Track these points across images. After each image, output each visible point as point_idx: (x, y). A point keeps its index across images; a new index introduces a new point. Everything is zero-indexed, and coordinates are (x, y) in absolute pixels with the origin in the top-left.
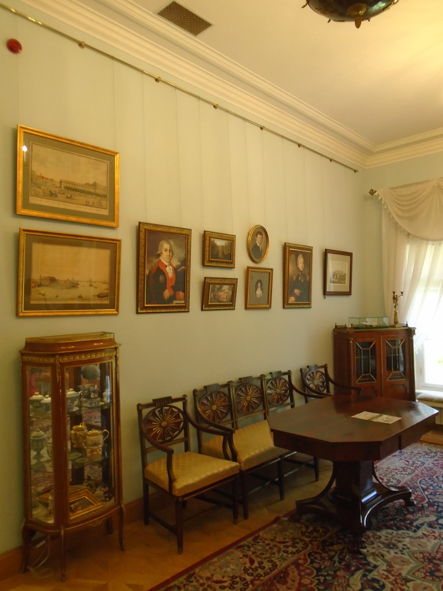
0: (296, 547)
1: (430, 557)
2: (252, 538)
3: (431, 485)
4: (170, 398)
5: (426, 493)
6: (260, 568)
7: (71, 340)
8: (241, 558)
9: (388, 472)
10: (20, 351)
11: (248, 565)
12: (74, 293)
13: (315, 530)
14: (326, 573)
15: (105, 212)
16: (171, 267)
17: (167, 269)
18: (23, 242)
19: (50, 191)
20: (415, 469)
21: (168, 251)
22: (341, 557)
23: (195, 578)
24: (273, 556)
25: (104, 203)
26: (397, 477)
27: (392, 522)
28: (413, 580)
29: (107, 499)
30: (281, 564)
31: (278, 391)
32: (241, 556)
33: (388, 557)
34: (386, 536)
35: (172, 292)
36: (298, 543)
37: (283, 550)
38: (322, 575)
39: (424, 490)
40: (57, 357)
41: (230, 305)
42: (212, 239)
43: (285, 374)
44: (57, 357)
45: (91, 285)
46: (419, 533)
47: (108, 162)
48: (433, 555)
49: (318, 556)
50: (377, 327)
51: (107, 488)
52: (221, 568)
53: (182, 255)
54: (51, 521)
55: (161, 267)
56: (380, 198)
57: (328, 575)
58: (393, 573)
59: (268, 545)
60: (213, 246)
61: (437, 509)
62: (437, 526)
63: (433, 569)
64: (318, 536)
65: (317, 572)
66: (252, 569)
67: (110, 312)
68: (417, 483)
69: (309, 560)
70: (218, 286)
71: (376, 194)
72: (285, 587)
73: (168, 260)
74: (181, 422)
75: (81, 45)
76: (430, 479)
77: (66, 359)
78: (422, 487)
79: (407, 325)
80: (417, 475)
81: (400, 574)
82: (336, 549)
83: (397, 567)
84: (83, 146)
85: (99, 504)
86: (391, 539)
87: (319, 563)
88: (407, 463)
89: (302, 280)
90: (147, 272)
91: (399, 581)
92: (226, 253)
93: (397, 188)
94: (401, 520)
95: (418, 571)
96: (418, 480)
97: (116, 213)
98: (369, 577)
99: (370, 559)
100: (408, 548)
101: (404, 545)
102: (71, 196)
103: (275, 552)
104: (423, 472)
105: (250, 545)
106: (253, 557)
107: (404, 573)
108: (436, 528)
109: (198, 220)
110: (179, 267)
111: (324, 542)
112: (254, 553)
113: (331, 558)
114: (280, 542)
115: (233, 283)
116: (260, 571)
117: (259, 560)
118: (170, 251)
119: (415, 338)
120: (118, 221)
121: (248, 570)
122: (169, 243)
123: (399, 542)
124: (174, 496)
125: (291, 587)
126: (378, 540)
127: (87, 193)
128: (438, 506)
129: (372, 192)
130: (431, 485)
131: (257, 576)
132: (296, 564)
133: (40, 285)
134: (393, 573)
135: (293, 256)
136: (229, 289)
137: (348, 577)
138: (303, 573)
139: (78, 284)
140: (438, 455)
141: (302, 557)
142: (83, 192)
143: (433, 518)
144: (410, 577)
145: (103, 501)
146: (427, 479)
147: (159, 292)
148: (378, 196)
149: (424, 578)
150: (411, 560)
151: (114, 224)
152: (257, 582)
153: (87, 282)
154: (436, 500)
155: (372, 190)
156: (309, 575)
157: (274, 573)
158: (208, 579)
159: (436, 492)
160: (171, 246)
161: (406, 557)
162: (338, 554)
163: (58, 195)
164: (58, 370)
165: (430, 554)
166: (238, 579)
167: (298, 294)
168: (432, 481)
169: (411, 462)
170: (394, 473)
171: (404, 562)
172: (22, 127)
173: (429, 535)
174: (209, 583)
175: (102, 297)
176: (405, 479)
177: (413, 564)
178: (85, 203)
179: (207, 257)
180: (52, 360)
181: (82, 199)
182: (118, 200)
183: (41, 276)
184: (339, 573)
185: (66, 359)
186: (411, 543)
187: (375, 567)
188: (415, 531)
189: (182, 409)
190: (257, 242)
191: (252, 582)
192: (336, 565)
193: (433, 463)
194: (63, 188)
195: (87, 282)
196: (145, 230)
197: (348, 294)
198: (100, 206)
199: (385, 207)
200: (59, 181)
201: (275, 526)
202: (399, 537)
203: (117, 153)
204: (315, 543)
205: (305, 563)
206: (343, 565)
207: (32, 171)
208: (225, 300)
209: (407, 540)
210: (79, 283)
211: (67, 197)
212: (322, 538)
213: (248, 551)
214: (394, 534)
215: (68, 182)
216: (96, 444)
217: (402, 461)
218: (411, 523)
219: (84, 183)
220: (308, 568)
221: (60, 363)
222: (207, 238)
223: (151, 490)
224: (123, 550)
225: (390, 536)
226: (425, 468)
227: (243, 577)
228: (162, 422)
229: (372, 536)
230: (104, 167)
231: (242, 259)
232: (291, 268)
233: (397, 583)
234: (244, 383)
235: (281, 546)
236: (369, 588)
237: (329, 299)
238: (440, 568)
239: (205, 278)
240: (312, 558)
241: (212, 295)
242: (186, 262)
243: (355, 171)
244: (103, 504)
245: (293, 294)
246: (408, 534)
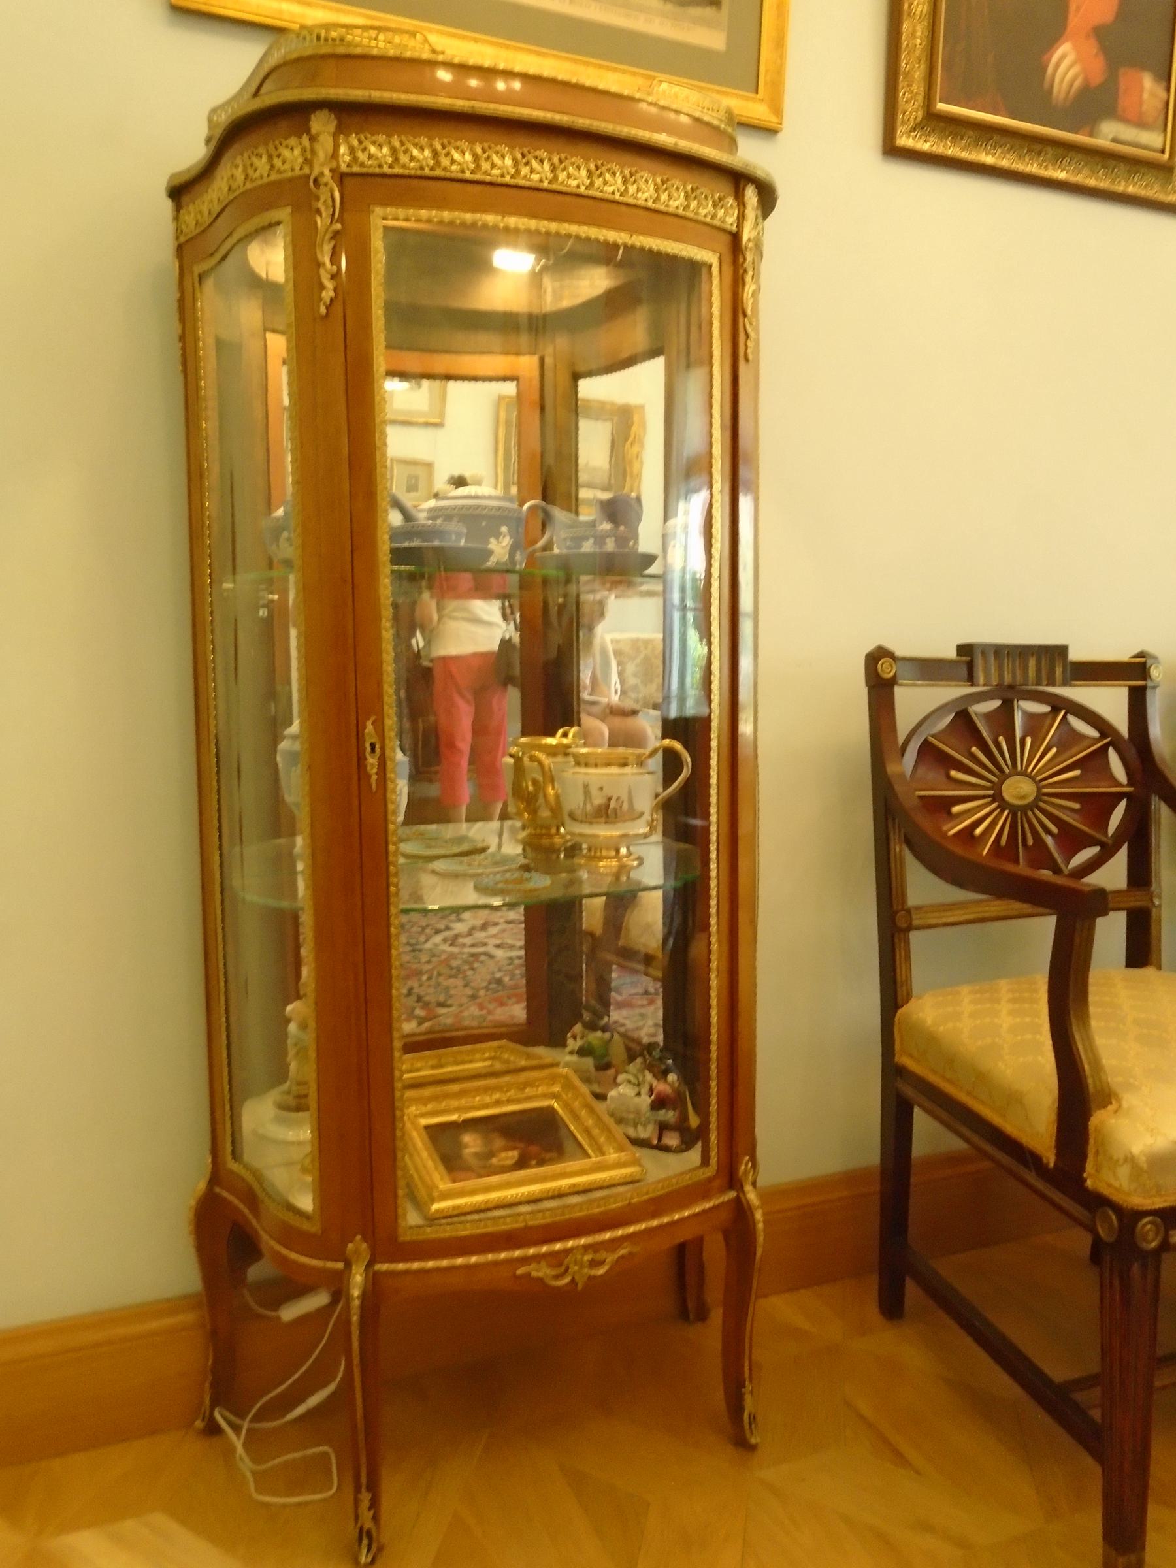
4: (1056, 653)
29: (672, 1140)
35: (1098, 69)
40: (322, 124)
51: (672, 1077)
54: (306, 1202)
74: (1113, 800)
85: (613, 1156)
124: (1098, 1202)
189: (1121, 722)
216: (606, 813)
221: (342, 178)
223: (928, 1135)
224: (742, 1444)
228: (1003, 776)
244: (636, 1162)
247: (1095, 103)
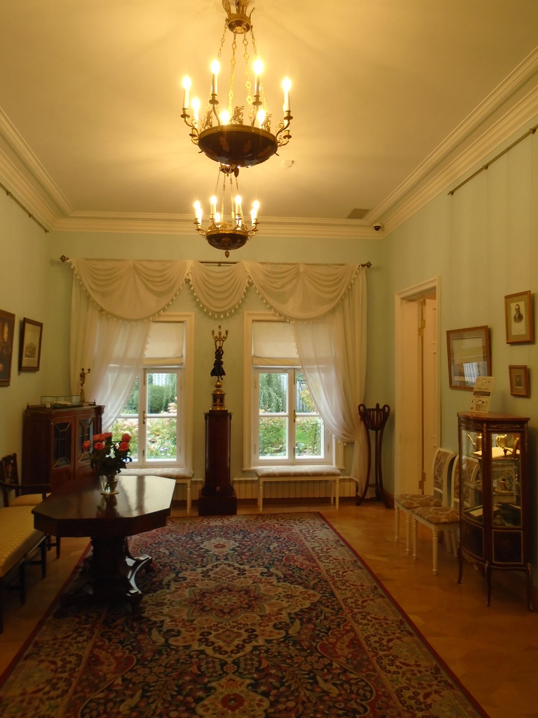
46: (173, 588)
56: (72, 267)
58: (178, 621)
71: (68, 261)
81: (183, 620)
91: (187, 624)
99: (153, 619)
100: (174, 601)
107: (185, 617)
129: (63, 259)
148: (70, 264)
149: (201, 615)
155: (63, 256)
177: (186, 610)
187: (162, 622)
199: (78, 277)
209: (168, 596)
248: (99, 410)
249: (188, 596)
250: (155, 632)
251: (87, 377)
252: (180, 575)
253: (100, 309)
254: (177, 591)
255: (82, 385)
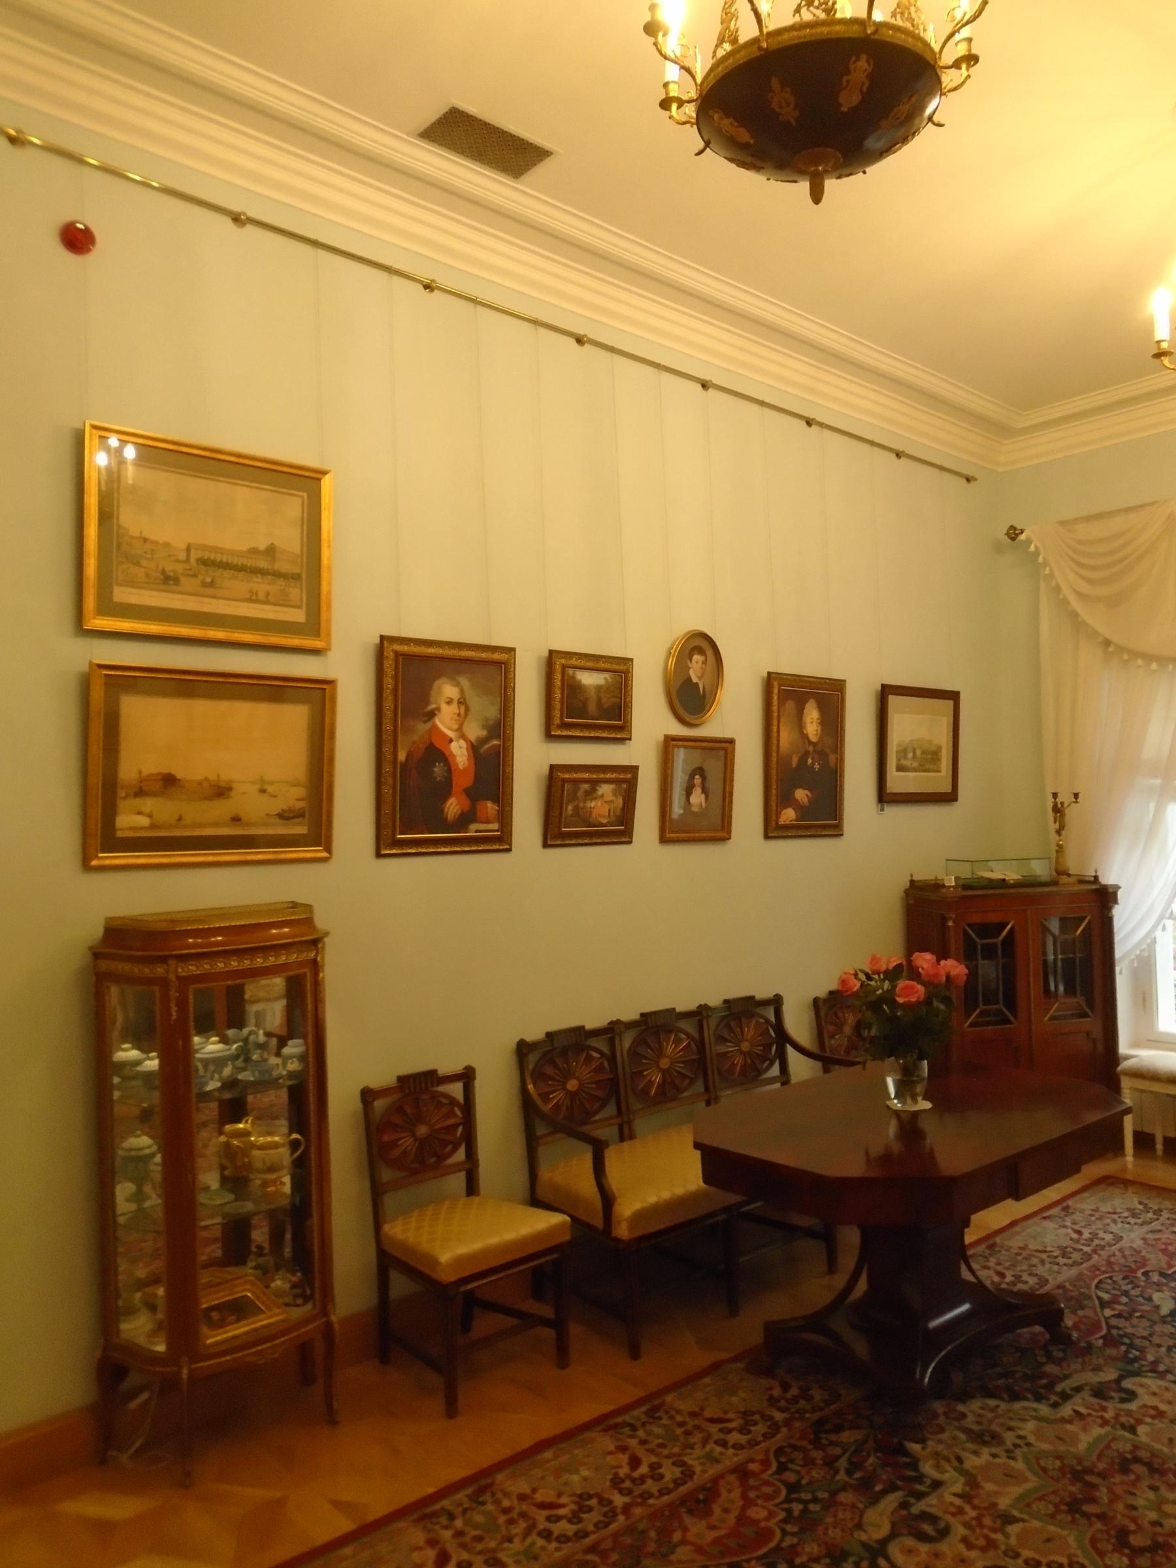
0: (749, 1432)
1: (1079, 1468)
2: (644, 1409)
3: (1126, 1294)
5: (1108, 1312)
6: (652, 1477)
7: (205, 922)
8: (610, 1453)
9: (1019, 1258)
10: (91, 948)
11: (623, 1471)
12: (222, 809)
13: (804, 1394)
14: (809, 1497)
15: (298, 616)
16: (462, 743)
17: (454, 747)
18: (98, 694)
19: (163, 572)
20: (1095, 1251)
21: (455, 705)
22: (854, 1460)
23: (493, 1494)
24: (689, 1451)
25: (296, 593)
26: (1041, 1270)
27: (1001, 1382)
28: (1023, 1520)
29: (299, 1301)
30: (704, 1471)
31: (745, 1046)
32: (612, 1448)
33: (973, 1462)
34: (980, 1415)
35: (467, 804)
36: (756, 1424)
37: (715, 1437)
38: (799, 1501)
39: (1103, 1304)
41: (620, 830)
42: (571, 672)
43: (765, 1003)
44: (172, 963)
45: (263, 791)
46: (1066, 1410)
47: (305, 495)
48: (1087, 1464)
49: (798, 1456)
50: (1018, 885)
51: (299, 1274)
52: (558, 1473)
53: (493, 712)
54: (161, 1348)
55: (438, 744)
57: (815, 1500)
58: (976, 1501)
59: (681, 1424)
60: (573, 689)
61: (1127, 1352)
62: (1113, 1394)
63: (1079, 1496)
64: (808, 1407)
65: (789, 1493)
66: (633, 1480)
67: (309, 855)
68: (1089, 1287)
69: (774, 1465)
70: (586, 786)
72: (704, 1523)
73: (456, 727)
75: (238, 219)
76: (1124, 1278)
77: (192, 969)
78: (1099, 1298)
79: (1096, 877)
80: (1095, 1268)
82: (845, 1440)
83: (989, 1487)
84: (241, 461)
85: (277, 1311)
86: (991, 1421)
87: (798, 1472)
88: (1075, 1236)
89: (817, 766)
90: (402, 756)
91: (987, 1521)
92: (607, 702)
93: (1077, 520)
94: (1026, 1377)
95: (1041, 1499)
96: (1093, 1278)
97: (324, 616)
98: (915, 1510)
99: (927, 1468)
100: (1028, 1445)
101: (1020, 1437)
102: (213, 581)
103: (695, 1444)
104: (1112, 1259)
105: (638, 1424)
106: (640, 1452)
108: (1112, 1398)
109: (533, 626)
110: (483, 741)
111: (820, 1423)
112: (643, 1442)
113: (830, 1462)
114: (712, 1420)
115: (626, 778)
116: (651, 1486)
117: (654, 1459)
118: (459, 703)
119: (1119, 914)
120: (329, 634)
121: (623, 1481)
122: (457, 684)
123: (1010, 1429)
125: (718, 1524)
126: (956, 1423)
127: (252, 572)
128: (1131, 1346)
130: (1126, 1294)
131: (640, 1496)
132: (742, 1473)
133: (140, 793)
134: (976, 1501)
135: (790, 706)
136: (614, 793)
137: (861, 1506)
138: (752, 1494)
139: (230, 789)
140: (1162, 1219)
141: (760, 1457)
142: (241, 569)
143: (1110, 1375)
144: (1016, 1513)
145: (287, 1305)
146: (1118, 1277)
147: (435, 802)
148: (1029, 542)
149: (1052, 1516)
150: (1028, 1474)
151: (318, 644)
152: (638, 1511)
153: (253, 782)
154: (1129, 1330)
156: (768, 1498)
157: (683, 1489)
158: (522, 1497)
159: (1135, 1311)
160: (462, 691)
161: (1019, 1465)
162: (847, 1455)
163: (183, 579)
164: (174, 994)
165: (1080, 1460)
166: (594, 1502)
167: (806, 800)
168: (1131, 1282)
169: (1086, 1235)
170: (1035, 1261)
171: (1011, 1476)
172: (95, 427)
173: (1089, 1415)
174: (524, 1507)
175: (289, 819)
176: (1057, 1276)
177: (1032, 1482)
178: (248, 596)
179: (557, 714)
180: (160, 970)
181: (241, 585)
182: (330, 584)
183: (140, 772)
184: (843, 1497)
185: (192, 969)
186: (1038, 1433)
187: (937, 1485)
188: (1055, 1405)
190: (691, 673)
191: (626, 1509)
192: (838, 1478)
193: (1144, 1239)
194: (193, 561)
195: (253, 782)
196: (396, 653)
197: (949, 797)
198: (284, 601)
200: (184, 546)
201: (707, 1380)
202: (1011, 1419)
203: (325, 473)
204: (797, 1424)
205: (763, 1471)
206: (857, 1479)
207: (119, 526)
208: (605, 821)
209: (1031, 1425)
210: (234, 786)
211: (204, 585)
212: (817, 1415)
213: (631, 1437)
214: (1000, 1411)
215: (204, 547)
217: (1063, 1231)
218: (1050, 1387)
219: (245, 548)
220: (767, 1483)
222: (557, 665)
225: (990, 1415)
226: (1121, 1250)
227: (606, 1496)
229: (945, 1414)
230: (293, 506)
231: (652, 718)
232: (786, 737)
233: (981, 1525)
234: (655, 1026)
235: (714, 1429)
236: (910, 1534)
237: (892, 811)
238: (1097, 1494)
239: (552, 767)
240: (783, 1460)
241: (570, 807)
242: (501, 729)
243: (968, 480)
245: (786, 800)
246: (1035, 1410)
247: (464, 820)
248: (1105, 897)
249: (1082, 1447)
250: (891, 1501)
251: (1071, 813)
252: (1128, 1384)
253: (1100, 640)
254: (1070, 1422)
255: (1059, 832)
